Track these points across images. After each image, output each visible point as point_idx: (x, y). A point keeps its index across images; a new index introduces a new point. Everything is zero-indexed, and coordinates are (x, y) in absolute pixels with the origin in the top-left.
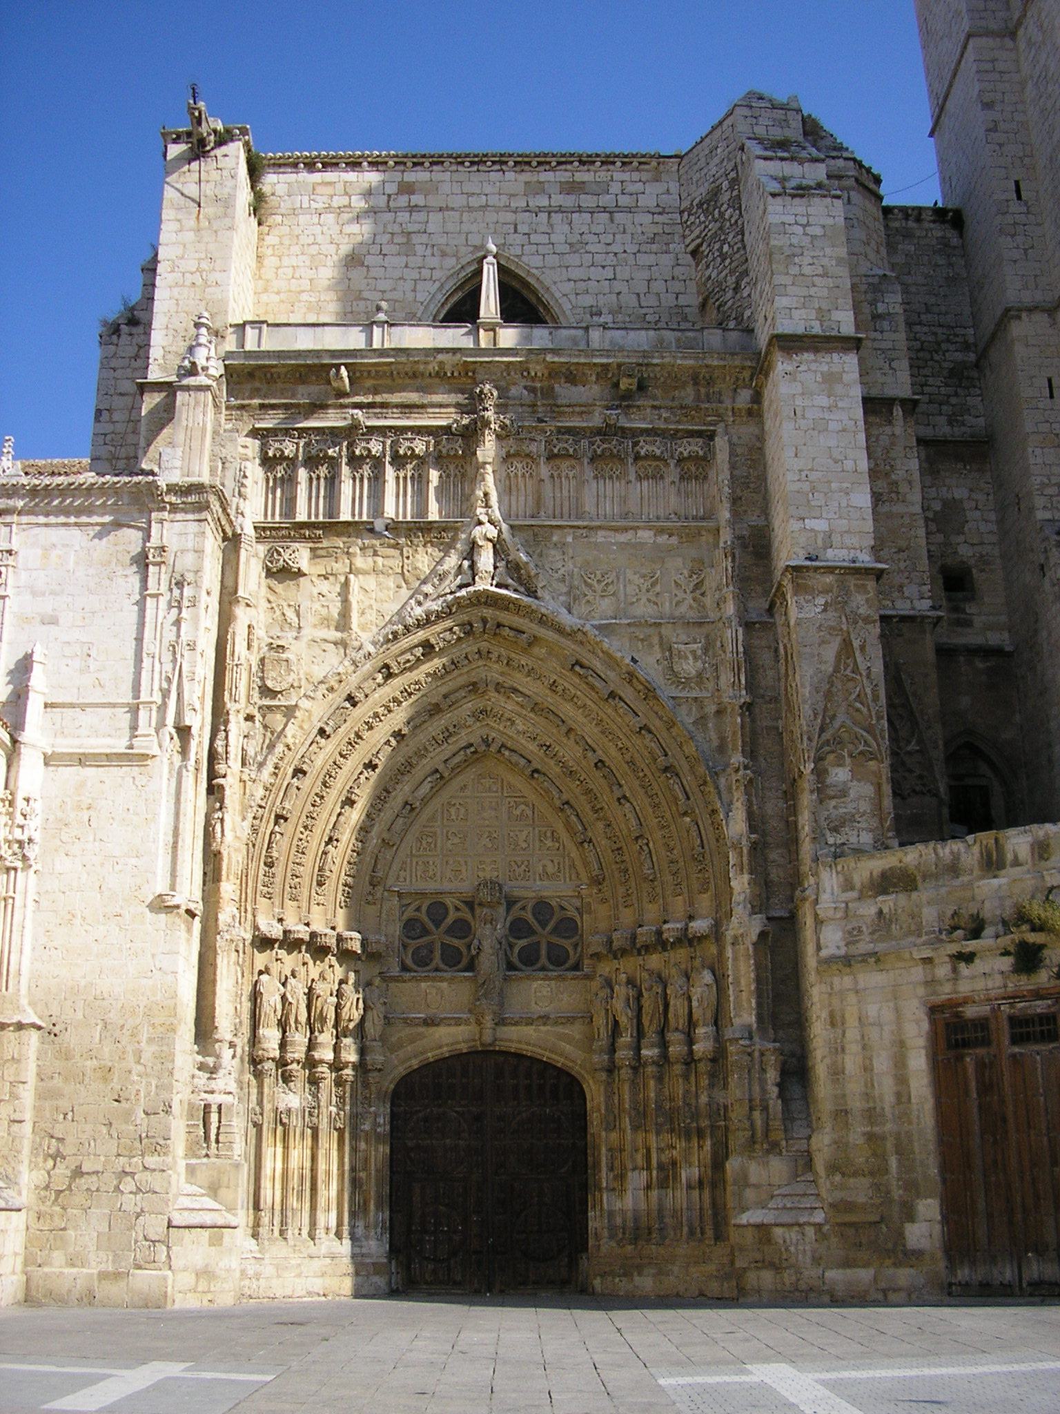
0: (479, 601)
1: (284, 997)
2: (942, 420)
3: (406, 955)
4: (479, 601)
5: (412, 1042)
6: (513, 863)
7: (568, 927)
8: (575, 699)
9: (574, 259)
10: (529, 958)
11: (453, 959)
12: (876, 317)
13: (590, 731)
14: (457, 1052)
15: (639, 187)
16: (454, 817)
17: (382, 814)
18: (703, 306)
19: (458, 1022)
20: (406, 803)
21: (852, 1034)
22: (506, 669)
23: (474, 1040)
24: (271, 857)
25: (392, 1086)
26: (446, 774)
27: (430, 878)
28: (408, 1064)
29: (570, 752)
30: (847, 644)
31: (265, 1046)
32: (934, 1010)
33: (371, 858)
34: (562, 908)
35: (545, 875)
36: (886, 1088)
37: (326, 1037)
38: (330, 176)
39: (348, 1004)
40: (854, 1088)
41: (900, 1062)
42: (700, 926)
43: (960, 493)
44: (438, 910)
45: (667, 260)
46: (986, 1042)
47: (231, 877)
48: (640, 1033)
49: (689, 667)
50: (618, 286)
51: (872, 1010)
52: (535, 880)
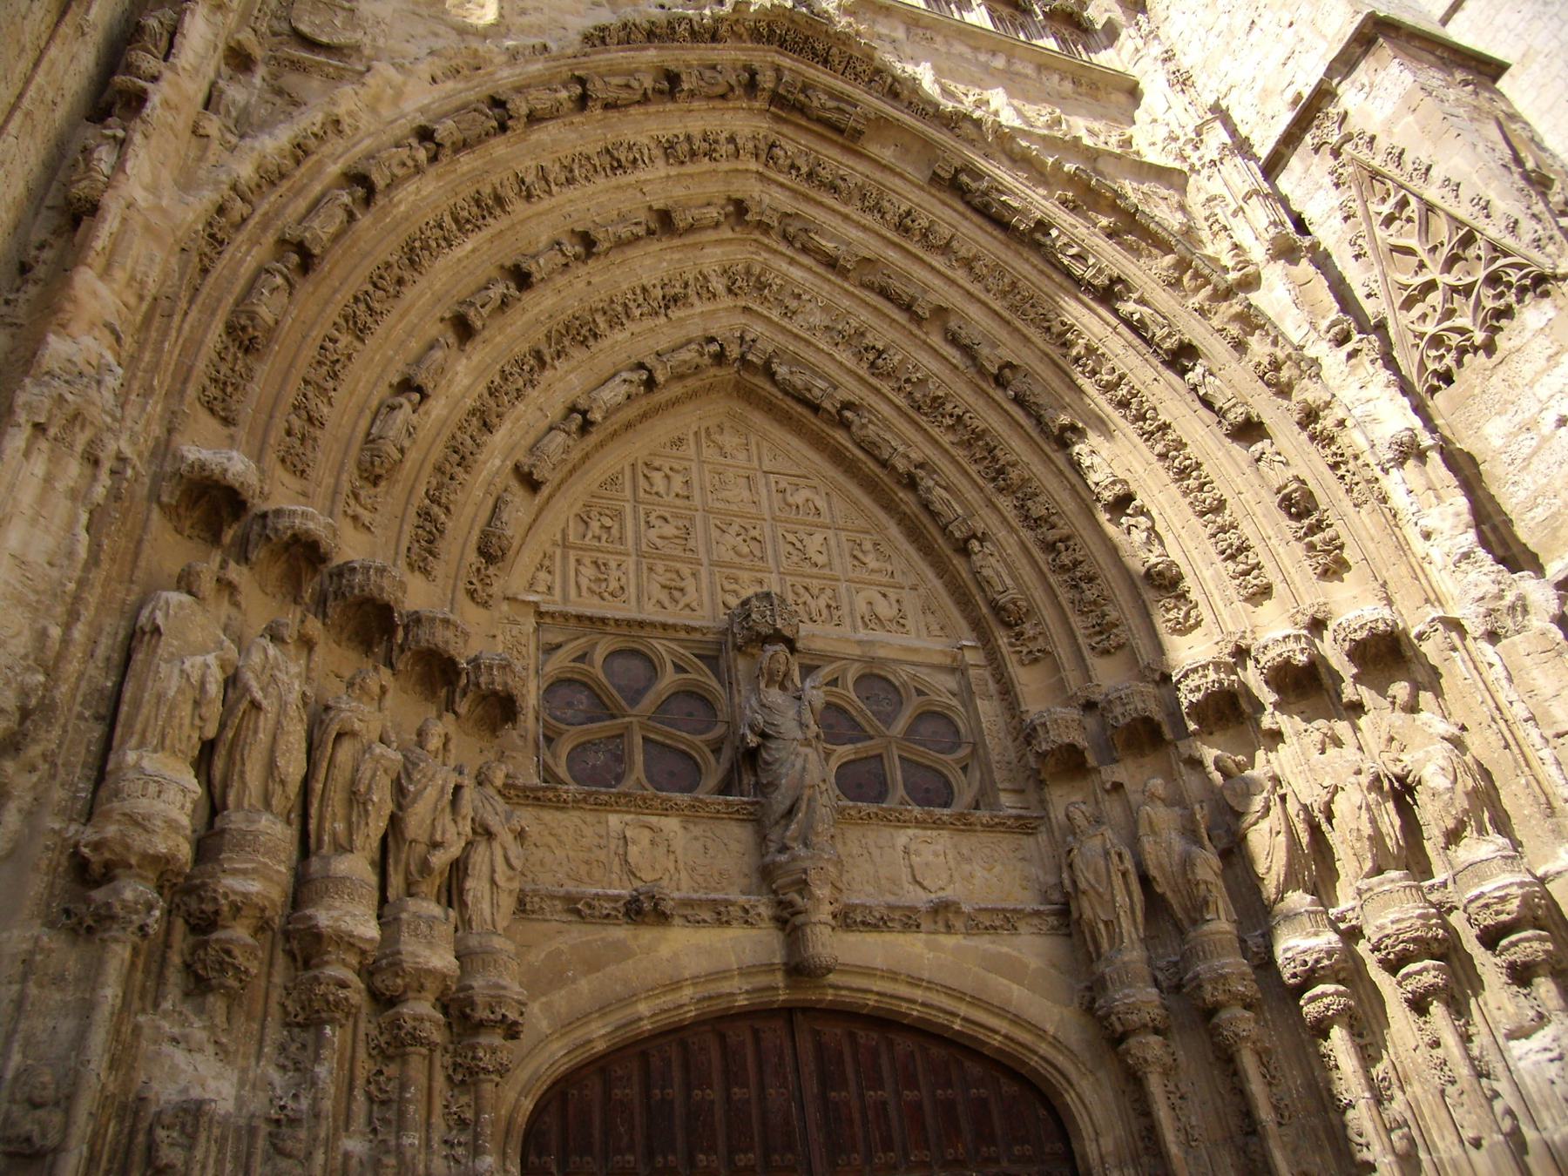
0: (772, 31)
1: (232, 681)
3: (555, 756)
4: (772, 31)
5: (593, 965)
6: (802, 591)
8: (955, 244)
14: (723, 1004)
16: (662, 490)
17: (521, 406)
19: (721, 914)
20: (573, 409)
22: (804, 187)
23: (769, 968)
24: (252, 316)
25: (528, 1105)
26: (660, 377)
27: (612, 594)
28: (579, 1034)
31: (143, 805)
33: (488, 492)
34: (920, 692)
37: (356, 866)
39: (431, 793)
47: (120, 275)
52: (855, 628)
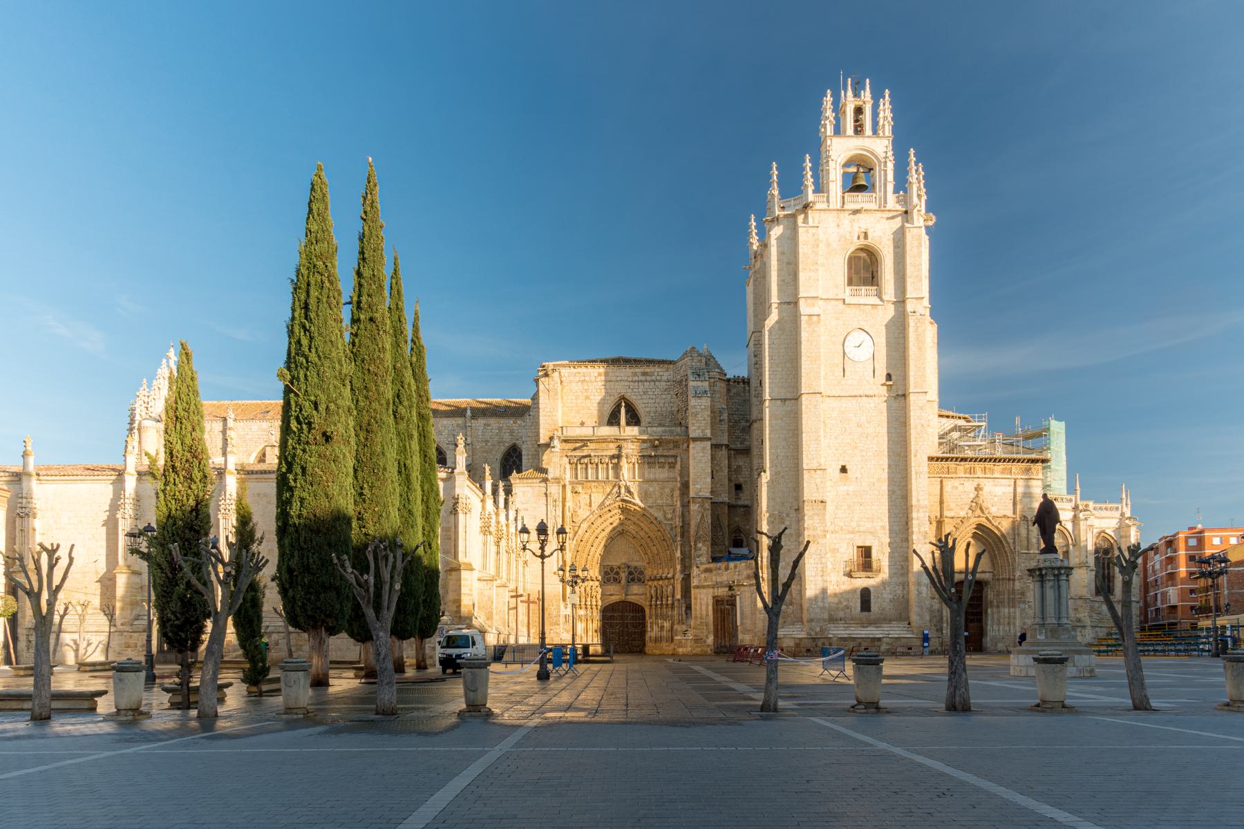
2: (738, 443)
7: (641, 573)
9: (644, 397)
10: (633, 580)
11: (615, 580)
12: (721, 421)
13: (647, 530)
15: (662, 373)
18: (678, 411)
21: (698, 601)
29: (642, 534)
30: (703, 515)
32: (714, 597)
35: (636, 561)
36: (704, 612)
38: (579, 370)
40: (698, 613)
41: (707, 607)
42: (670, 576)
43: (741, 463)
44: (612, 569)
45: (669, 396)
46: (722, 604)
48: (657, 598)
49: (669, 516)
50: (656, 405)
51: (702, 597)
